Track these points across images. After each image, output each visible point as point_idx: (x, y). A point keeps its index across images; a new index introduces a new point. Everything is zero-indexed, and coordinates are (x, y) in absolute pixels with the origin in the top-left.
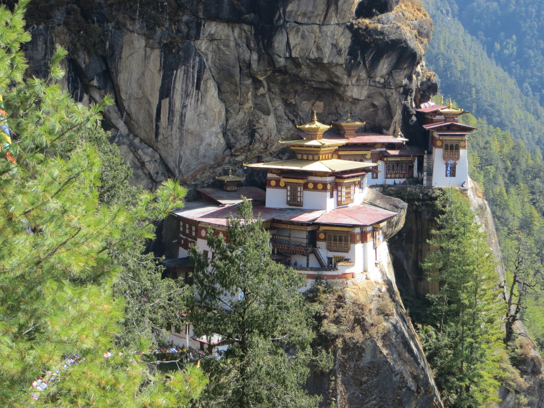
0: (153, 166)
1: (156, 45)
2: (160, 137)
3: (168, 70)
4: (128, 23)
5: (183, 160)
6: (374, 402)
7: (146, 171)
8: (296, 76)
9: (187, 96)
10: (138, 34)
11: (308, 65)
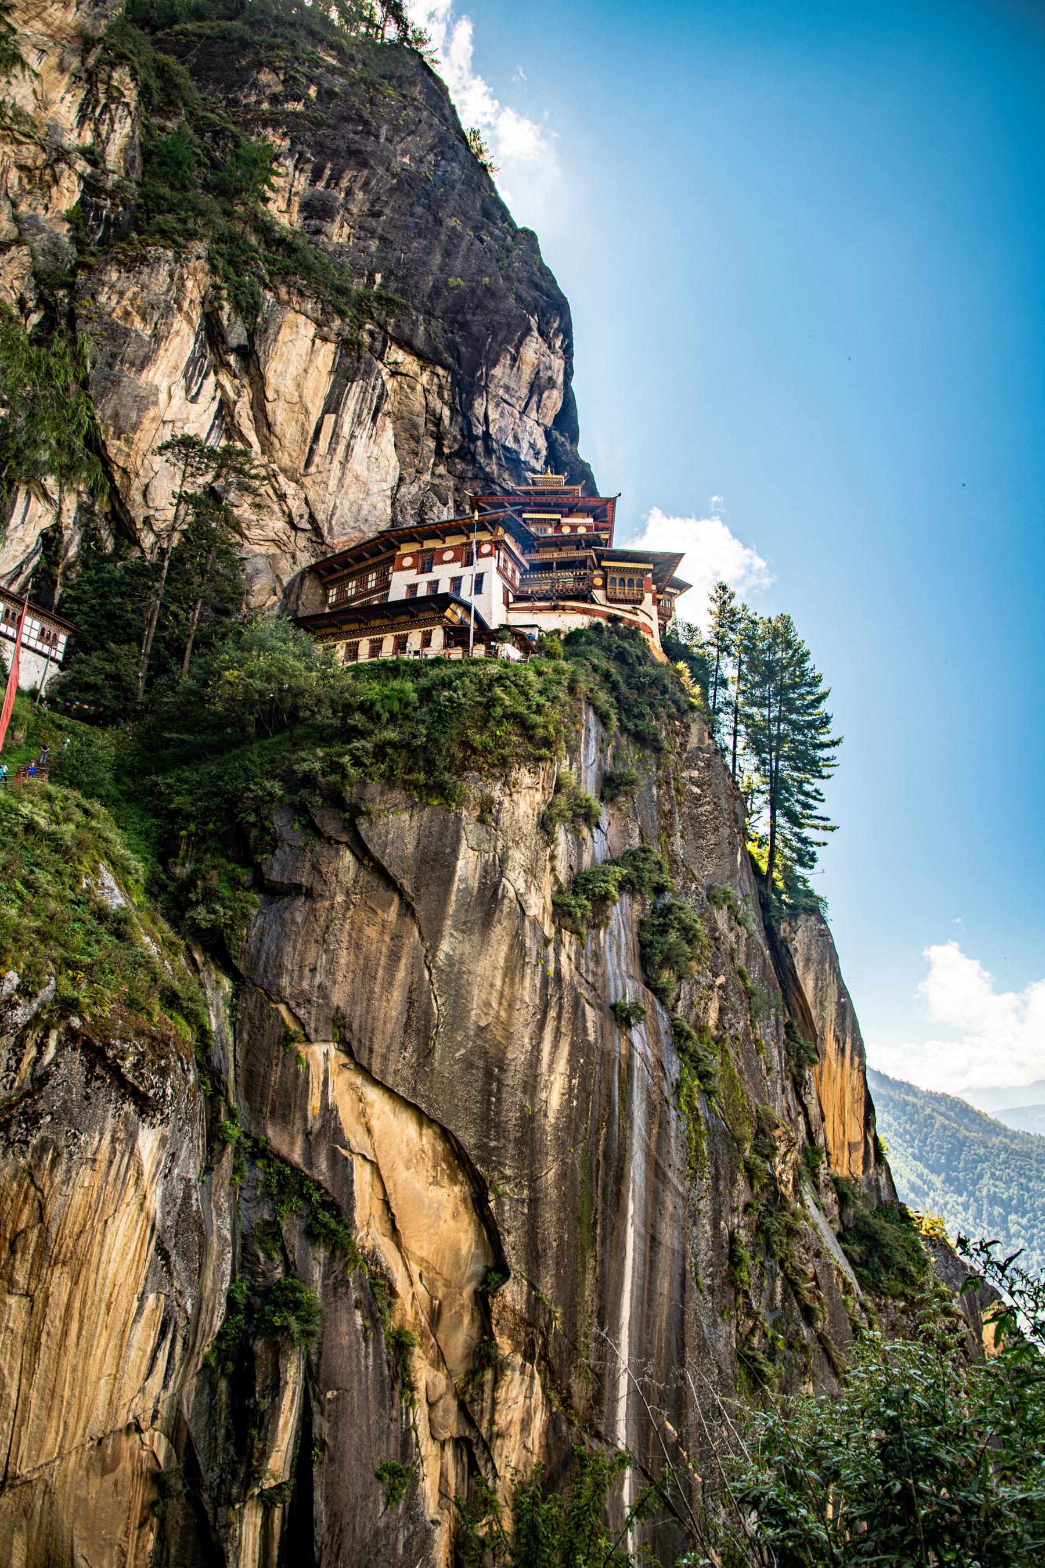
0: (297, 503)
1: (333, 337)
2: (313, 469)
3: (344, 375)
4: (294, 299)
5: (338, 513)
6: (708, 808)
7: (285, 508)
8: (481, 468)
9: (360, 423)
10: (307, 317)
11: (499, 459)
